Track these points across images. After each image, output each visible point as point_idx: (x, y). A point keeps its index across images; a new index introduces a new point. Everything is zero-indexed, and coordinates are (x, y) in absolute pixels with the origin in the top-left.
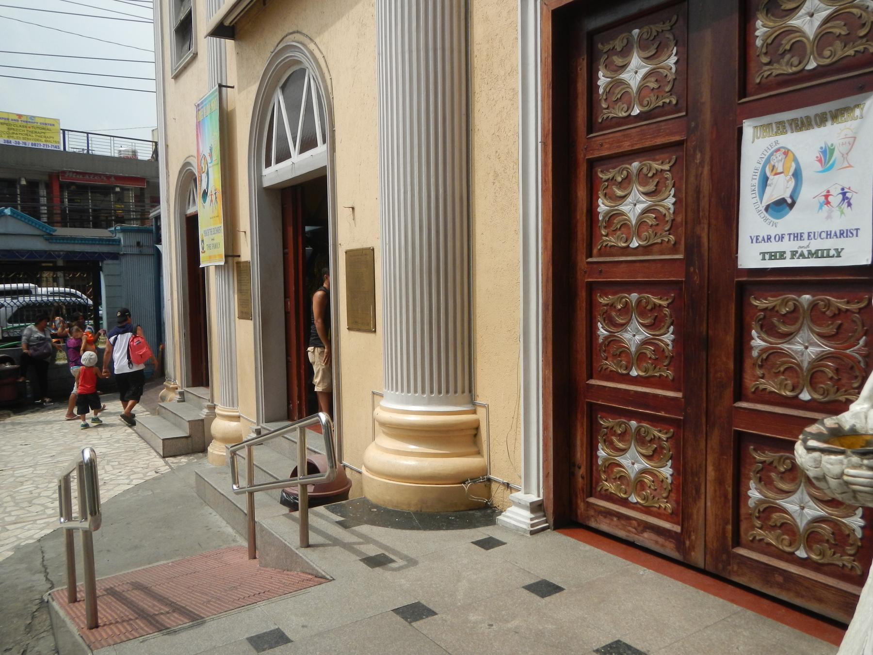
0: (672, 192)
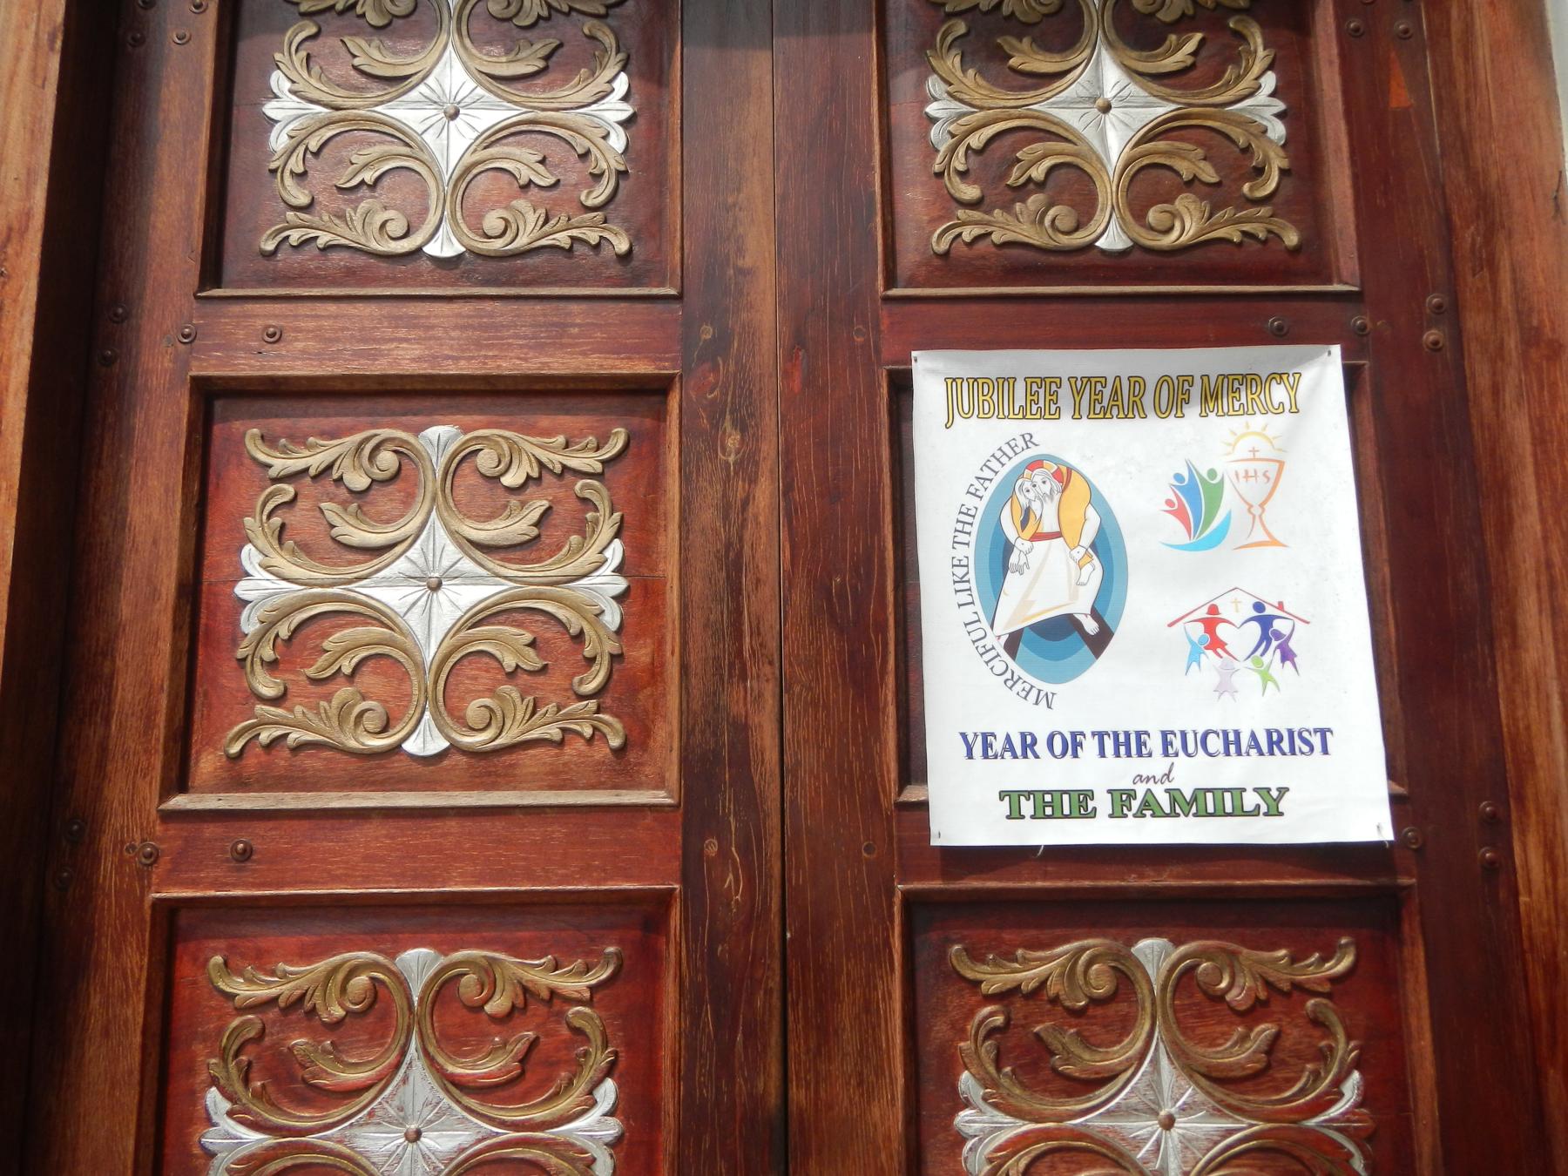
0: (616, 552)
